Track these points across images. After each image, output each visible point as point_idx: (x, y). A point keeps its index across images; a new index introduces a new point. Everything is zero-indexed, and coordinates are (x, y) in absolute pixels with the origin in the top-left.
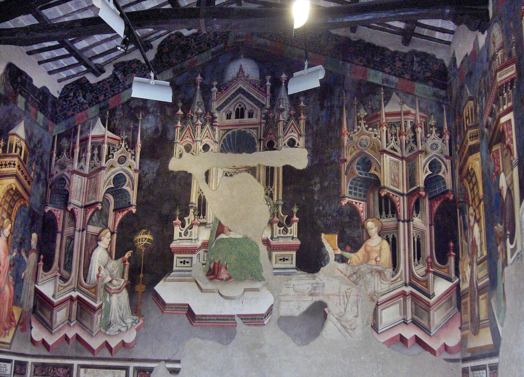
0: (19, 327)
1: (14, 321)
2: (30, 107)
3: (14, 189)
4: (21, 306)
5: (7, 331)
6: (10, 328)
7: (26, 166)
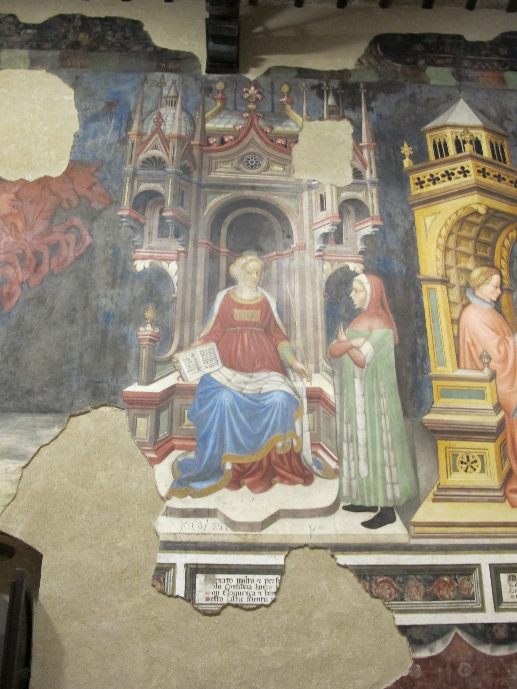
2: (472, 73)
3: (482, 210)
7: (508, 165)
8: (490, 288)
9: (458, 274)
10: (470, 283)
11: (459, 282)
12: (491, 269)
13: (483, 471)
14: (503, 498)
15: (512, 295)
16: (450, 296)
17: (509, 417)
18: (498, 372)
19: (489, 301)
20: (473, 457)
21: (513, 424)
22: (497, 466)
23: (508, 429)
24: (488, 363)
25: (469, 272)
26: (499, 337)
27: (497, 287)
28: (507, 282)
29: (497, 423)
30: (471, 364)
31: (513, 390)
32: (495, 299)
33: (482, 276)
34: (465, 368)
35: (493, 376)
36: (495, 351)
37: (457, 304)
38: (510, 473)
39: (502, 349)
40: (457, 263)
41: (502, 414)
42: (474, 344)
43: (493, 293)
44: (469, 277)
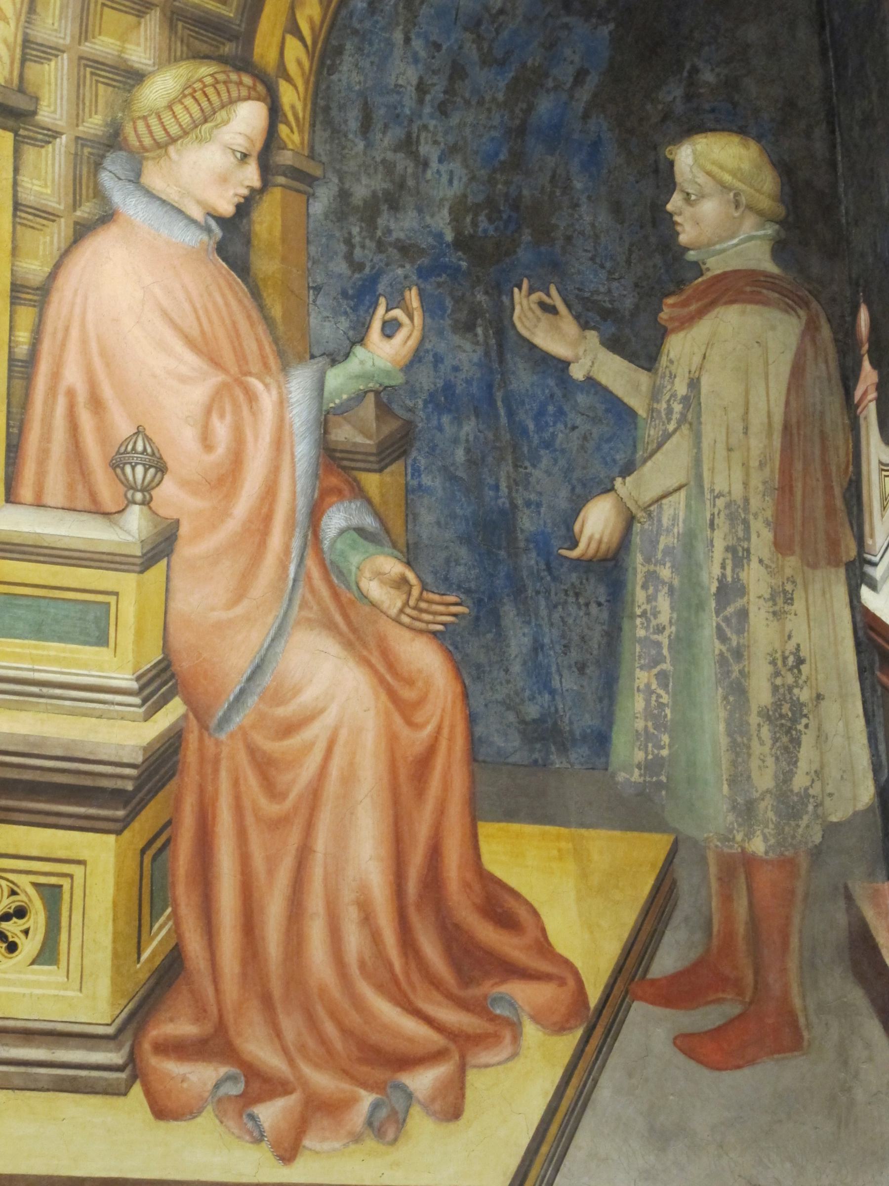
0: (649, 1029)
1: (564, 972)
4: (636, 812)
5: (423, 1081)
6: (461, 1046)
8: (213, 162)
9: (79, 85)
10: (129, 129)
11: (77, 119)
12: (234, 77)
13: (48, 954)
14: (123, 1075)
15: (311, 196)
16: (25, 180)
17: (204, 727)
18: (184, 530)
19: (197, 213)
20: (13, 893)
21: (217, 761)
22: (117, 937)
23: (190, 777)
24: (147, 489)
25: (132, 77)
26: (219, 378)
27: (245, 156)
28: (296, 138)
29: (145, 749)
30: (71, 487)
31: (239, 610)
32: (227, 208)
33: (189, 101)
34: (39, 504)
35: (162, 546)
36: (188, 437)
37: (50, 216)
38: (171, 969)
39: (222, 430)
40: (84, 34)
41: (173, 711)
42: (96, 403)
43: (224, 179)
44: (127, 104)
